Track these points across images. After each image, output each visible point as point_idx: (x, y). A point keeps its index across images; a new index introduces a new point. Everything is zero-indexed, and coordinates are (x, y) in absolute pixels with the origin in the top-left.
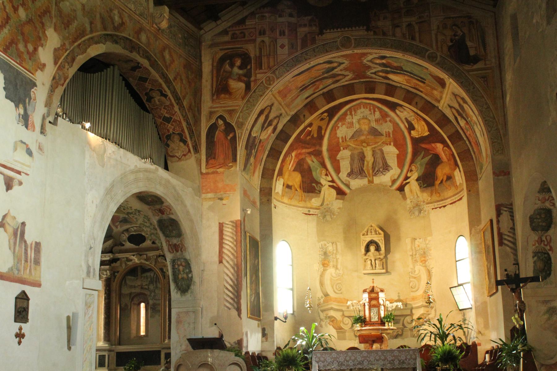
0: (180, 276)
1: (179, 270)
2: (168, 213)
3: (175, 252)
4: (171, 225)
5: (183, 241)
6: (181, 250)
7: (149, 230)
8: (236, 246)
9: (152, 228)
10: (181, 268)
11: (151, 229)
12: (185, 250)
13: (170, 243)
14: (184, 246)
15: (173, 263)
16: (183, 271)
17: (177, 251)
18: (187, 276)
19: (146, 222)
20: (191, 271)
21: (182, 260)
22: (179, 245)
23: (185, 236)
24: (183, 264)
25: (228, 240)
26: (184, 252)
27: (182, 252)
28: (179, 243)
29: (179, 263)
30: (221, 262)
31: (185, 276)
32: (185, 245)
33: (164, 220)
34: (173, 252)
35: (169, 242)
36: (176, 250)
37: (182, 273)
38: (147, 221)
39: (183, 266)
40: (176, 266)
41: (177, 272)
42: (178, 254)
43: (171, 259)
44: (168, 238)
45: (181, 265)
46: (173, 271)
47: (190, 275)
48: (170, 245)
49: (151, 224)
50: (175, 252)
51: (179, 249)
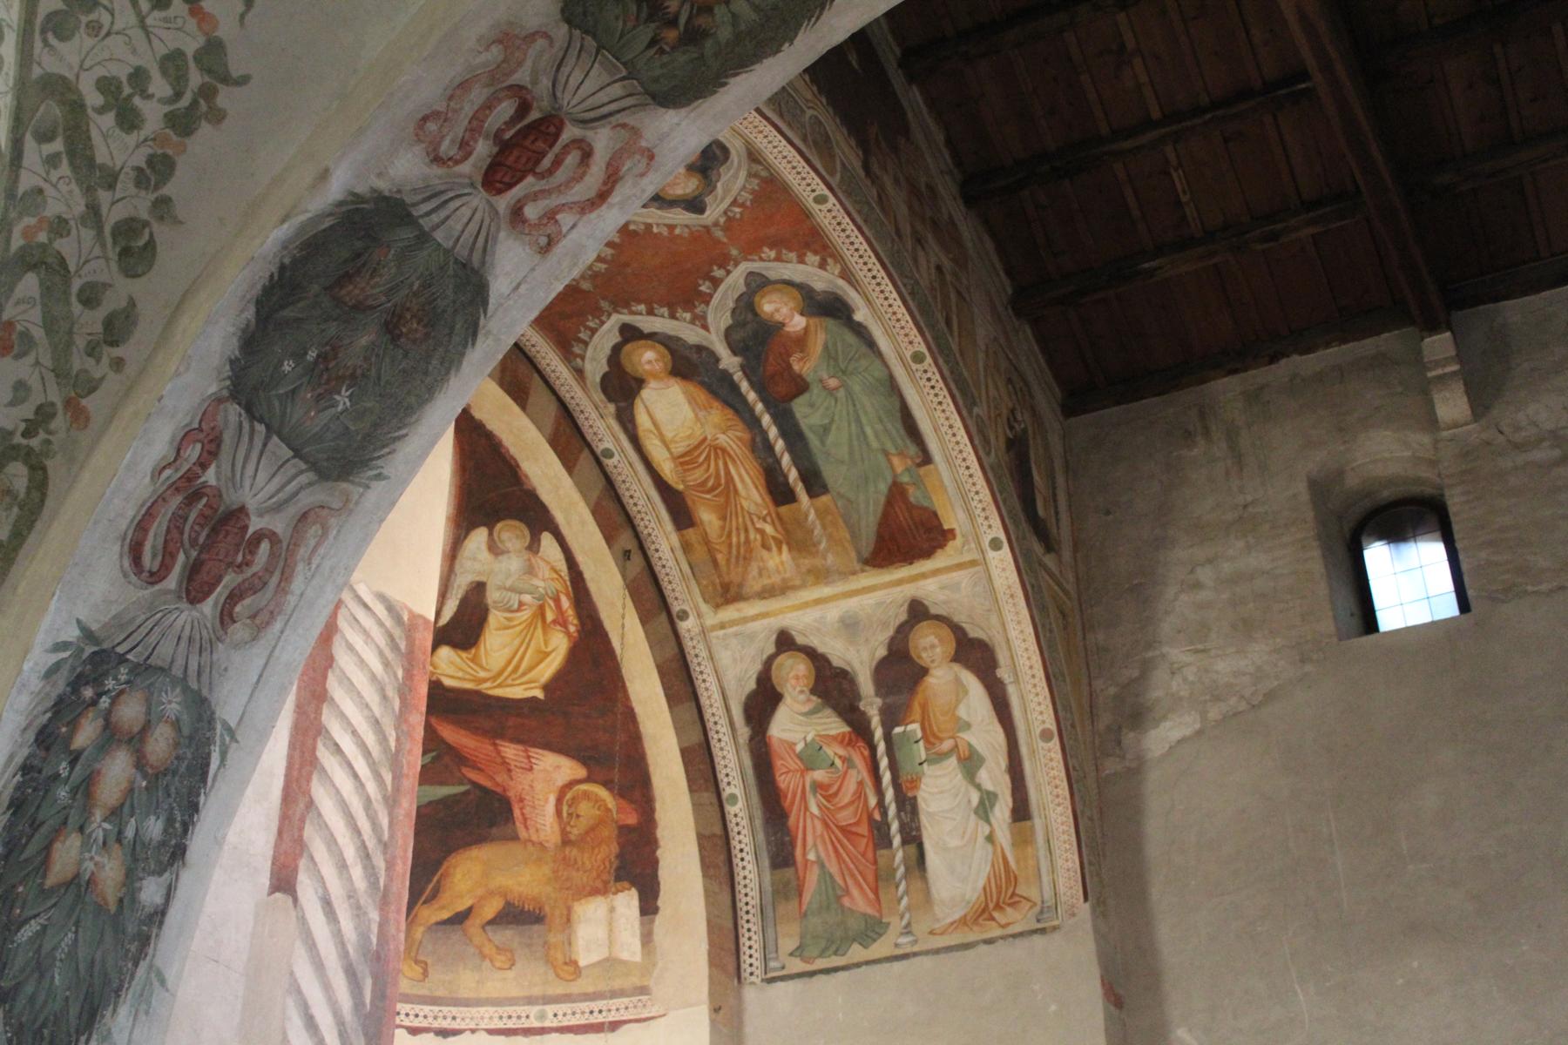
0: (67, 855)
1: (86, 788)
2: (531, 212)
3: (171, 582)
4: (392, 328)
5: (313, 531)
6: (234, 597)
7: (64, 198)
8: (391, 802)
9: (113, 216)
10: (117, 771)
11: (93, 213)
12: (260, 622)
13: (210, 476)
14: (286, 577)
15: (76, 684)
16: (115, 814)
17: (195, 588)
18: (131, 878)
19: (128, 120)
20: (174, 853)
21: (172, 703)
22: (259, 537)
23: (378, 487)
24: (159, 744)
25: (354, 733)
26: (239, 631)
27: (226, 616)
28: (279, 524)
29: (130, 712)
30: (283, 882)
31: (109, 871)
32: (297, 584)
33: (424, 238)
34: (156, 577)
35: (212, 449)
36: (193, 570)
37: (99, 825)
38: (152, 114)
39: (140, 763)
40: (87, 733)
41: (62, 793)
42: (184, 617)
43: (88, 635)
44: (234, 411)
45: (136, 740)
46: (26, 768)
47: (151, 892)
48: (190, 489)
49: (159, 168)
50: (171, 582)
51: (230, 580)
